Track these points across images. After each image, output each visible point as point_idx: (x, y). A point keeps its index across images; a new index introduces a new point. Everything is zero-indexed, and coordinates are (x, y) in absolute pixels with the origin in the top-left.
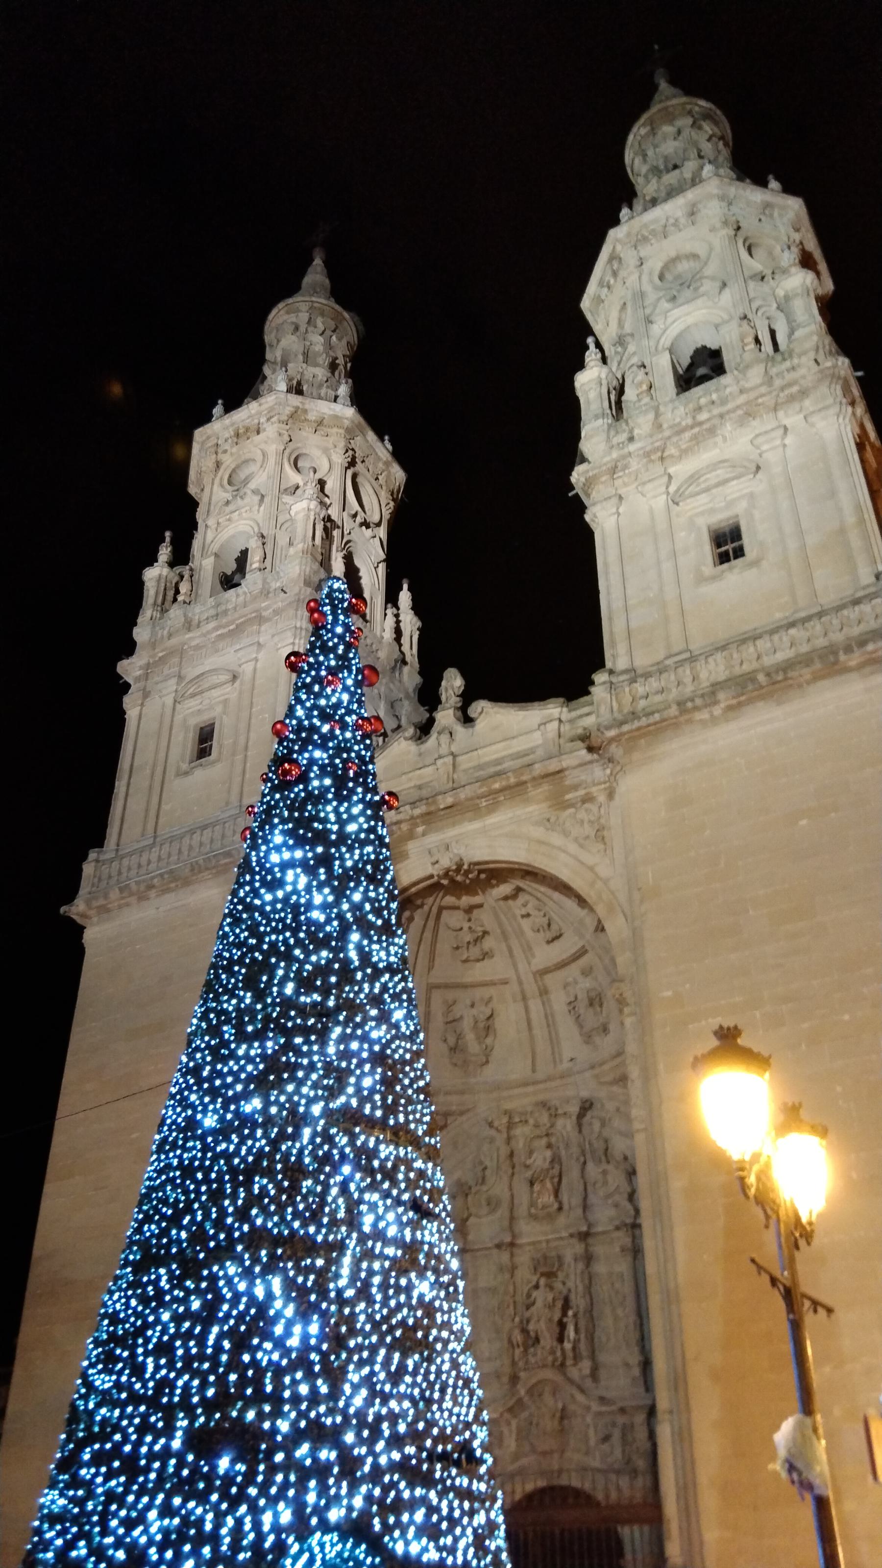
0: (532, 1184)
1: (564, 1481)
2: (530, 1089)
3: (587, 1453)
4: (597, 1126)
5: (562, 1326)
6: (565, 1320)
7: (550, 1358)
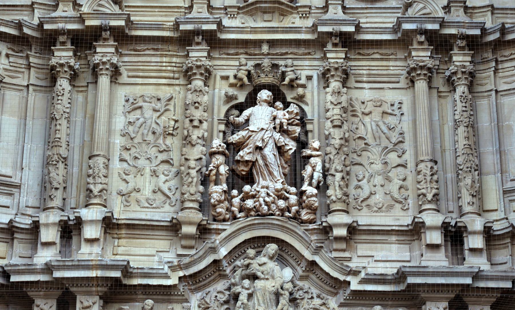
6: (307, 152)
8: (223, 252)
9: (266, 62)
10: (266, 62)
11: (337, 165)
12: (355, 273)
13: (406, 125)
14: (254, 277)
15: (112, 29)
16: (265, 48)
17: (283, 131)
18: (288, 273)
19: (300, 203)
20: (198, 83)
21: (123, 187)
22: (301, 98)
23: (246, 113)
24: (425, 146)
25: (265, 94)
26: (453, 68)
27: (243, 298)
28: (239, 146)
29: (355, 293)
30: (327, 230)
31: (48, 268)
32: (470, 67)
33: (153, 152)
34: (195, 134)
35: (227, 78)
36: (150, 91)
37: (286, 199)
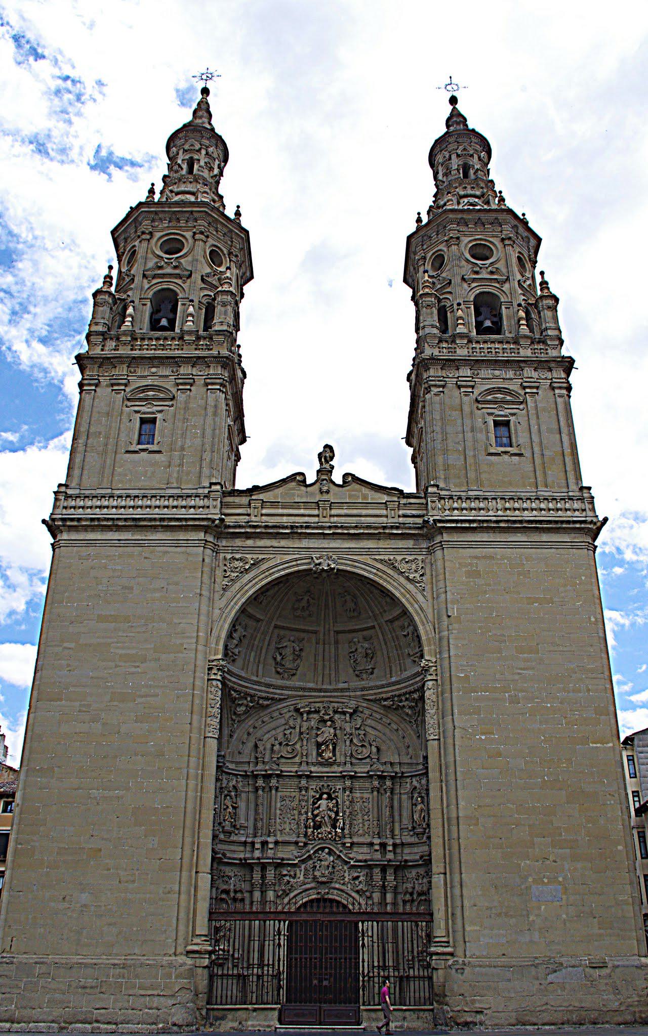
0: (319, 745)
1: (330, 896)
2: (322, 694)
3: (343, 884)
4: (359, 721)
5: (336, 820)
7: (330, 836)
8: (312, 852)
9: (326, 785)
10: (326, 785)
11: (347, 822)
12: (352, 859)
13: (370, 806)
14: (321, 860)
15: (276, 774)
16: (325, 778)
17: (330, 810)
18: (332, 858)
19: (336, 835)
20: (304, 792)
21: (280, 828)
22: (337, 796)
23: (319, 802)
24: (376, 815)
25: (325, 796)
26: (385, 787)
27: (318, 867)
28: (317, 815)
29: (352, 865)
30: (344, 844)
31: (258, 859)
32: (391, 786)
33: (289, 815)
34: (303, 811)
35: (312, 789)
36: (288, 794)
37: (331, 834)
